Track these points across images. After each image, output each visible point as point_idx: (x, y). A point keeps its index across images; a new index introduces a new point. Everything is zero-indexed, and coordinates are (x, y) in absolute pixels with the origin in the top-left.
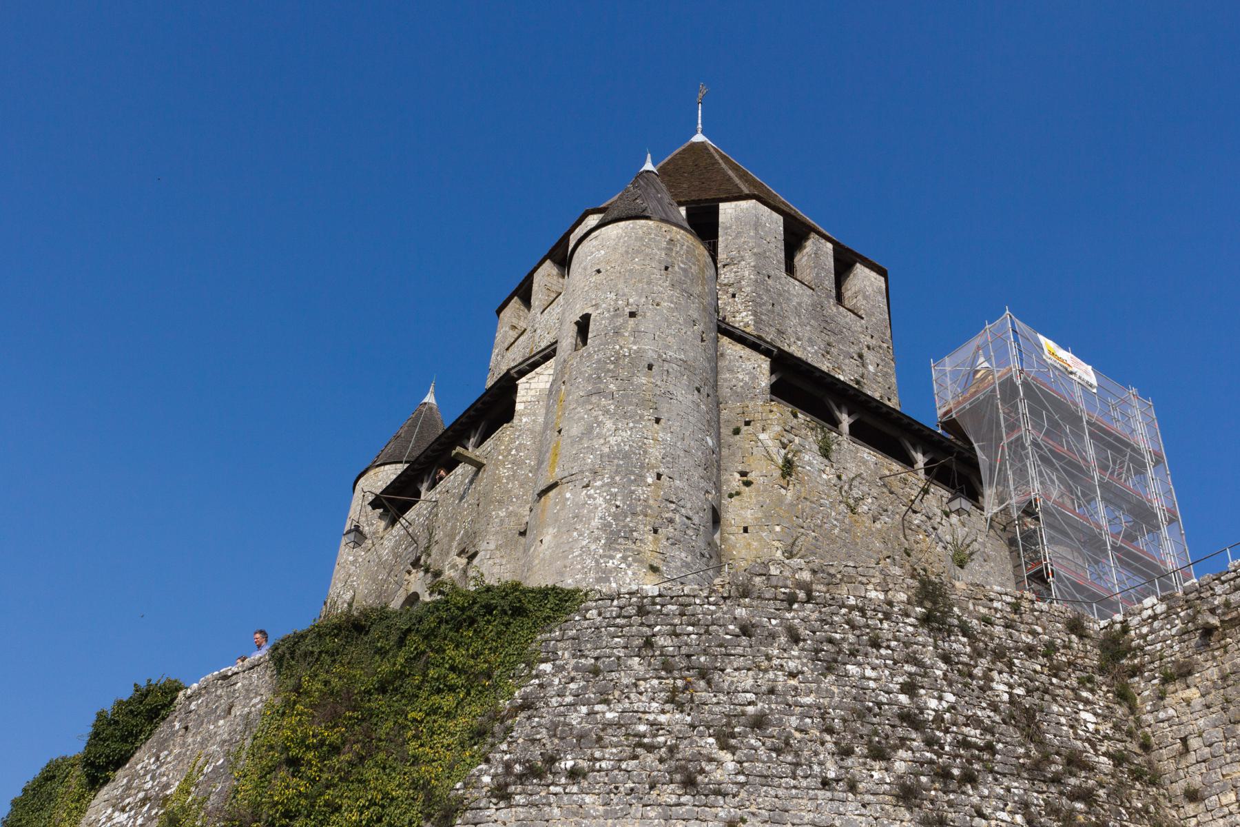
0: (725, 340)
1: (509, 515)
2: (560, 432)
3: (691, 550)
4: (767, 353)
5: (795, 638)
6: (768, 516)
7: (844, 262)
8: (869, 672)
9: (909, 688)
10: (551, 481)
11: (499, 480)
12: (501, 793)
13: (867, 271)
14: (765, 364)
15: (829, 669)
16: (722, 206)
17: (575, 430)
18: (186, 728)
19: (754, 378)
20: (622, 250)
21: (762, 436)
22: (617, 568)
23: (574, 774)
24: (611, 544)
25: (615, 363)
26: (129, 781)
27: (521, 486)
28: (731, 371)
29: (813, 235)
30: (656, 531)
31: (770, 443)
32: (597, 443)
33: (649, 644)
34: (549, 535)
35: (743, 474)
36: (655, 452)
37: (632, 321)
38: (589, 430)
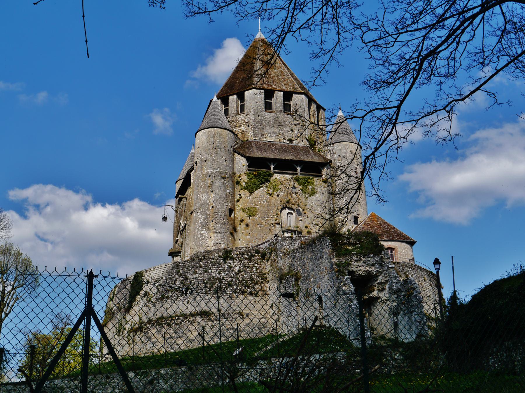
0: (236, 154)
3: (222, 224)
4: (245, 157)
5: (201, 267)
7: (288, 96)
8: (213, 271)
9: (219, 273)
13: (297, 95)
15: (206, 272)
16: (246, 93)
22: (204, 233)
28: (238, 164)
29: (276, 92)
30: (213, 221)
33: (179, 272)
35: (240, 195)
36: (212, 201)
37: (205, 163)
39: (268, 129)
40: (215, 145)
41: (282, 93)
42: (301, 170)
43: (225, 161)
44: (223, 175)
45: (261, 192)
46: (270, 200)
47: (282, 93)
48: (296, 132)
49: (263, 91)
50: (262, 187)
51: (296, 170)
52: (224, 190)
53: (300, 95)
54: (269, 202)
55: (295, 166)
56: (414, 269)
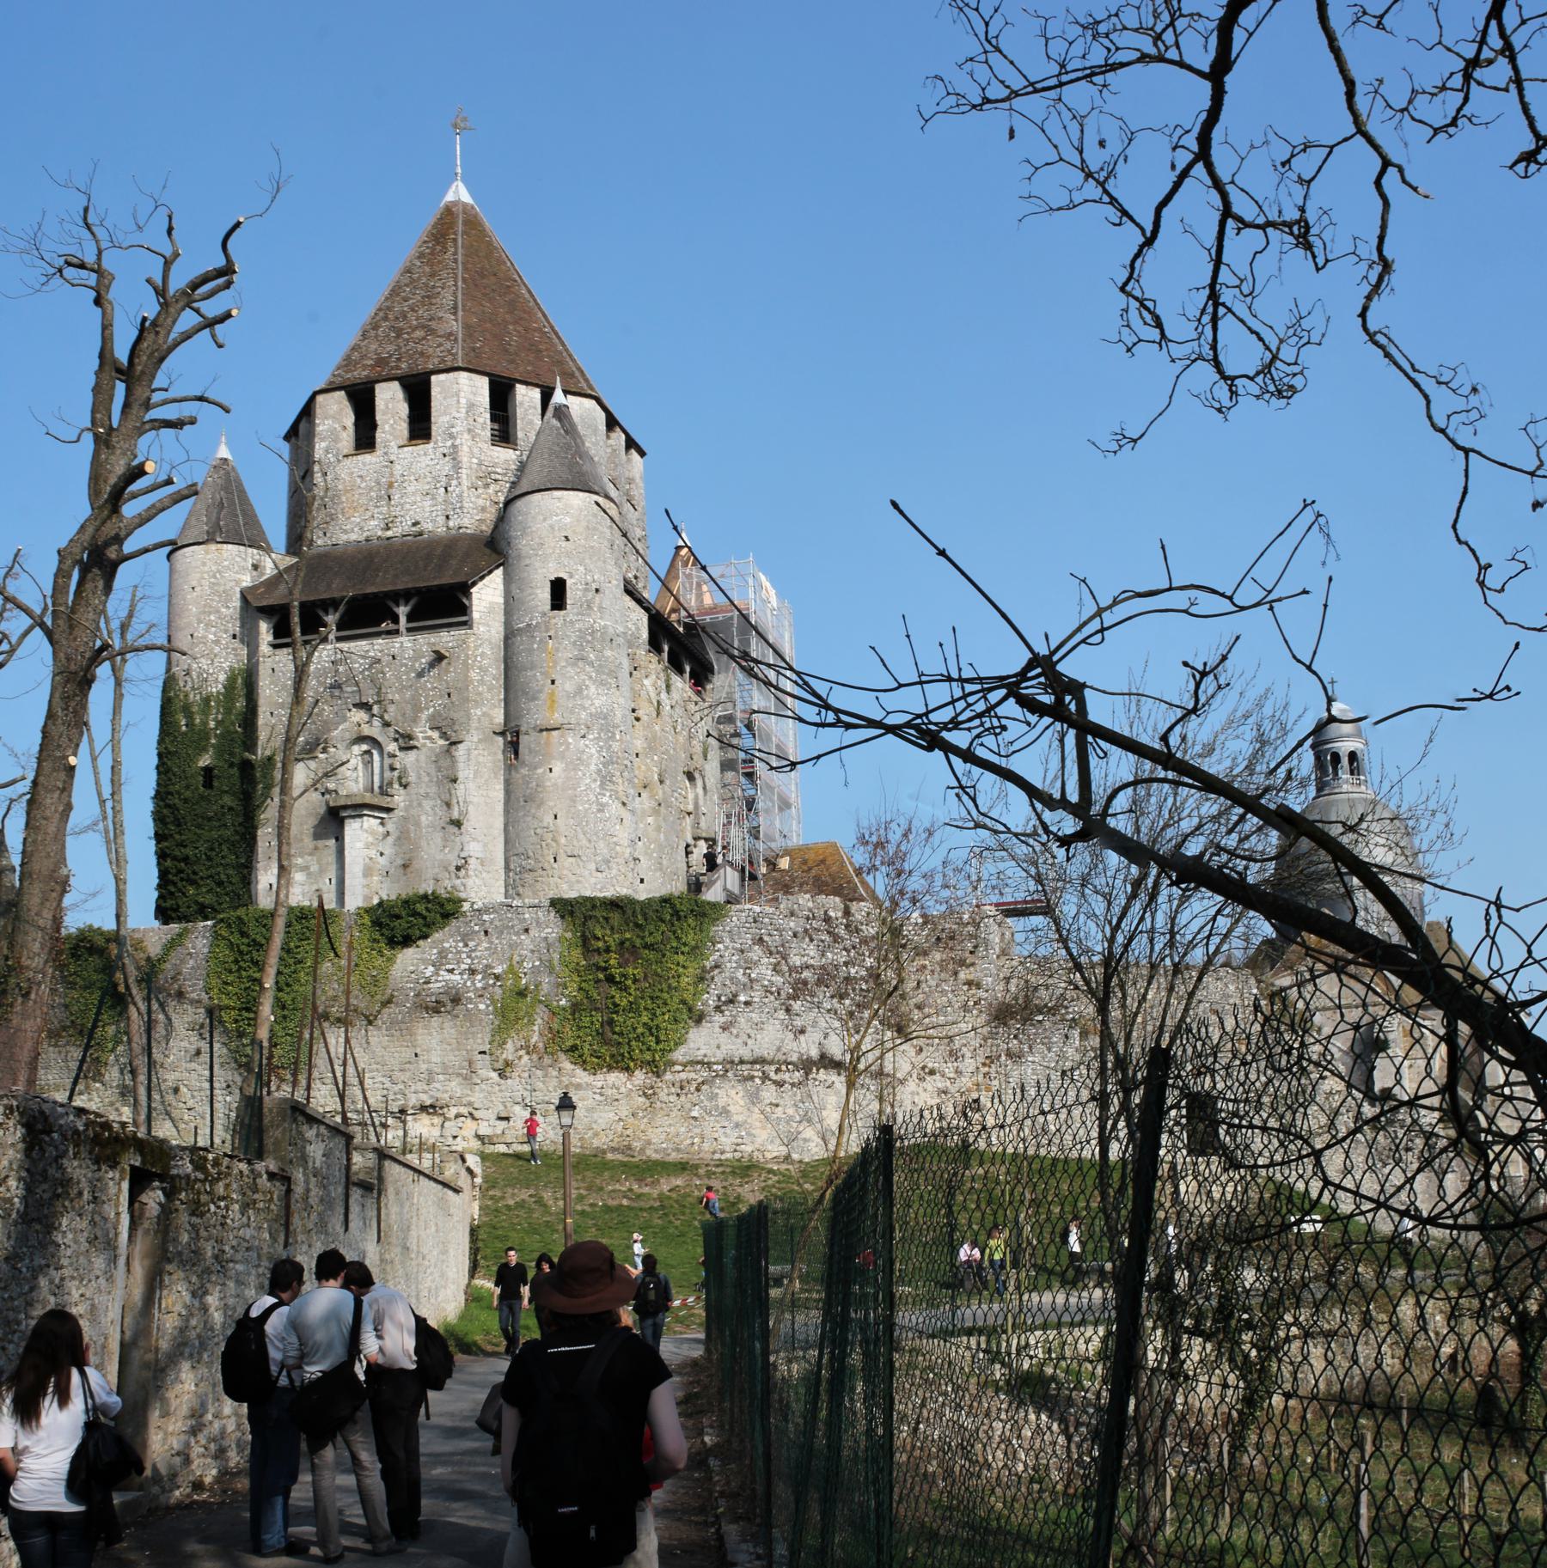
1: (484, 714)
2: (553, 682)
4: (647, 609)
6: (650, 748)
10: (552, 723)
11: (472, 682)
12: (718, 1009)
14: (643, 618)
17: (569, 686)
18: (486, 932)
19: (638, 629)
20: (584, 524)
21: (646, 682)
23: (747, 1003)
24: (602, 786)
25: (591, 634)
26: (439, 953)
27: (490, 690)
31: (651, 689)
32: (587, 703)
34: (558, 768)
37: (598, 597)
38: (579, 691)
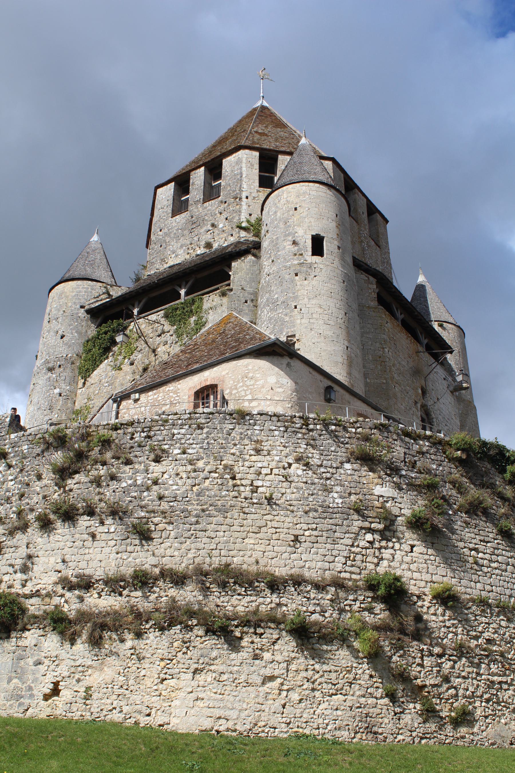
7: (214, 169)
39: (174, 245)
40: (50, 316)
41: (203, 169)
42: (187, 294)
43: (62, 337)
44: (51, 365)
45: (104, 369)
46: (116, 378)
47: (203, 169)
48: (221, 226)
49: (173, 183)
50: (107, 358)
51: (179, 297)
52: (48, 391)
53: (234, 155)
54: (112, 384)
55: (177, 288)
56: (200, 427)
